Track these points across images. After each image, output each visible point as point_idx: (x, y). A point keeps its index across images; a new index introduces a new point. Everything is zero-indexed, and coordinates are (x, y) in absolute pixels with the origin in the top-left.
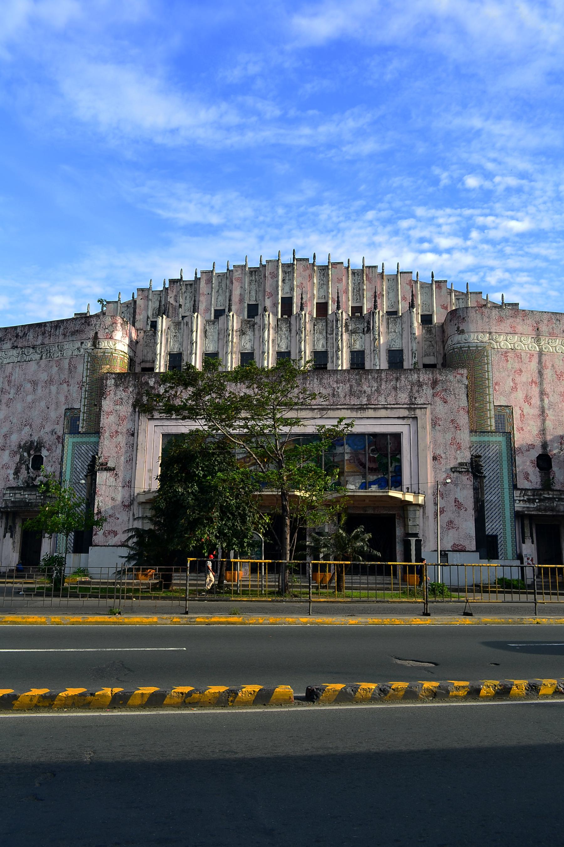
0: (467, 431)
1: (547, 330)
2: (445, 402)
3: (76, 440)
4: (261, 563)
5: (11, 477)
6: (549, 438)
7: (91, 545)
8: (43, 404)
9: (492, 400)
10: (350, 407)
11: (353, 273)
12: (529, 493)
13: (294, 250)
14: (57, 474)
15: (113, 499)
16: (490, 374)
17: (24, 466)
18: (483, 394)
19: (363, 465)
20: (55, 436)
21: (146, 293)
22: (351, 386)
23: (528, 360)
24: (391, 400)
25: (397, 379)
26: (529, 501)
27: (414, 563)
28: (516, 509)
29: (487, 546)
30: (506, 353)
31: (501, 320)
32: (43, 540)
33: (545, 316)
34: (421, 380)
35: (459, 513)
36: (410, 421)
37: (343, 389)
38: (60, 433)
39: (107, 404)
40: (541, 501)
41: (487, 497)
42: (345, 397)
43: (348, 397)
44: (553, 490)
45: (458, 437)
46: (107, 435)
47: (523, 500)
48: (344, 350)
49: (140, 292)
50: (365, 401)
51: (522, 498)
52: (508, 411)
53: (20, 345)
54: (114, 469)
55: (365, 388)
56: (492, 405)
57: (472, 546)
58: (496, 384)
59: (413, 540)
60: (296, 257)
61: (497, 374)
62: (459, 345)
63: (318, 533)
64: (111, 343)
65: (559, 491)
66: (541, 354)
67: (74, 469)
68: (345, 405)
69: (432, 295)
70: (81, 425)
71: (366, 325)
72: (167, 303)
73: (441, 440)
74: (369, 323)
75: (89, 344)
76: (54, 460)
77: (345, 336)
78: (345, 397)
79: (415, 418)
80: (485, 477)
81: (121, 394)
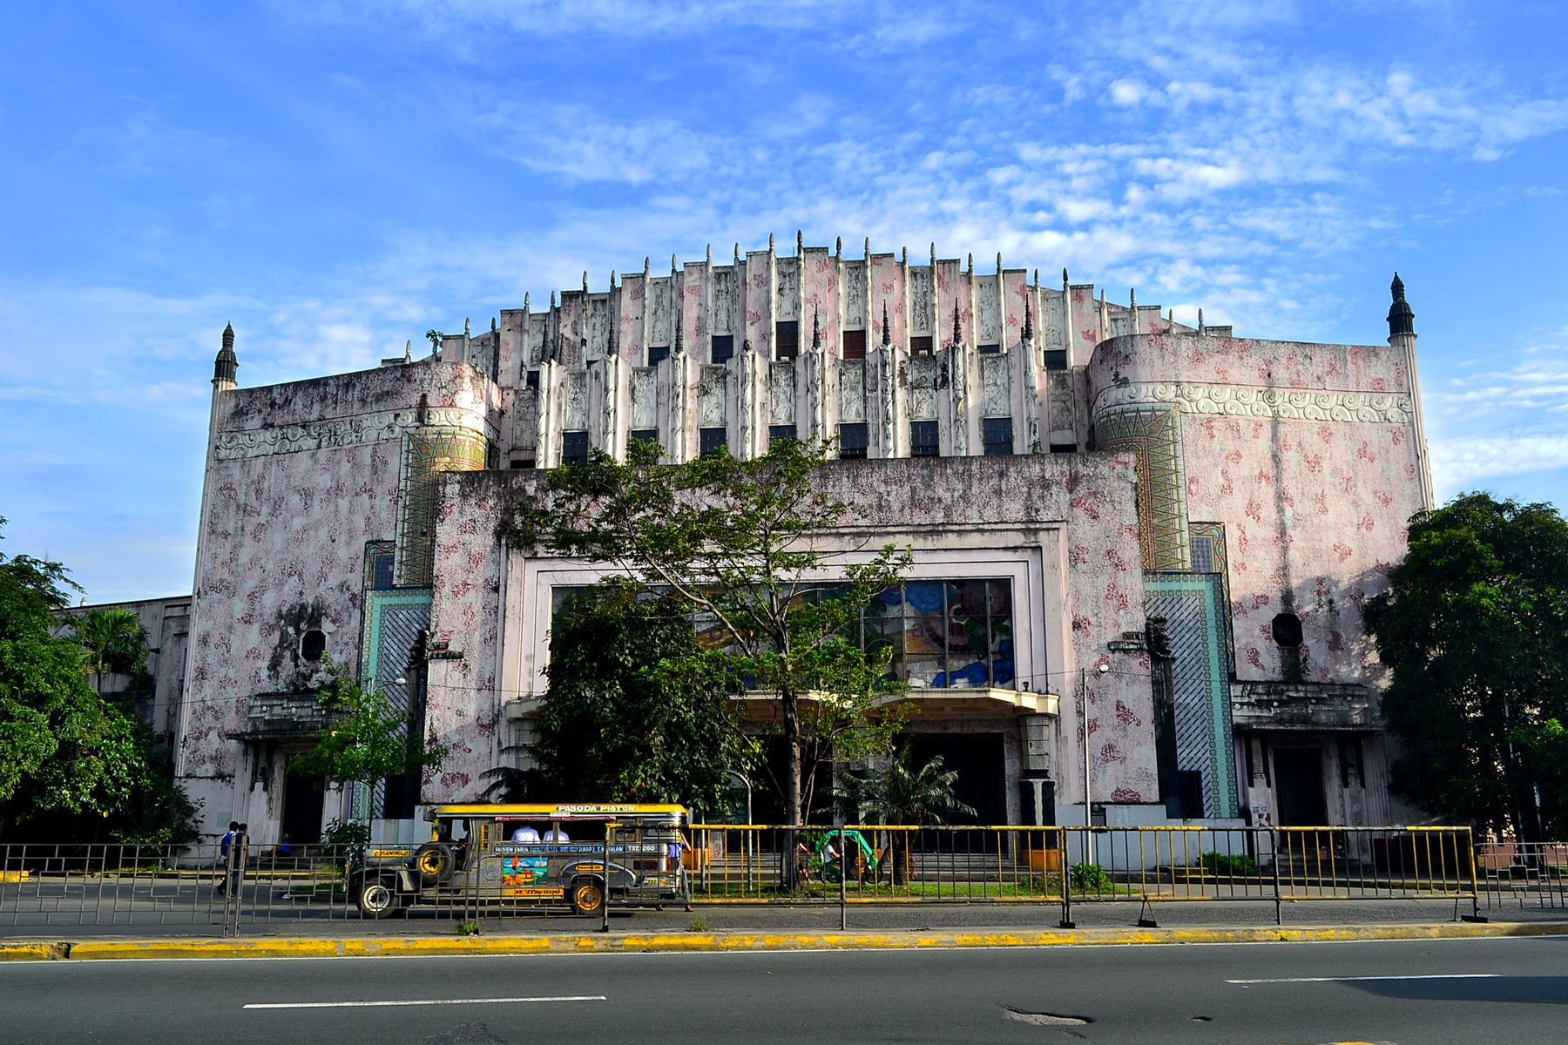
0: (1138, 572)
3: (387, 601)
4: (746, 831)
5: (264, 674)
6: (1295, 582)
7: (419, 803)
8: (323, 533)
9: (1183, 512)
11: (914, 274)
12: (1260, 689)
14: (353, 666)
15: (459, 713)
16: (1180, 462)
17: (288, 654)
18: (1167, 500)
19: (939, 641)
20: (347, 595)
21: (518, 319)
22: (913, 490)
24: (990, 514)
25: (1002, 475)
26: (1260, 704)
27: (1040, 826)
28: (1235, 720)
29: (1181, 793)
30: (1209, 421)
31: (1198, 358)
32: (327, 794)
33: (1283, 350)
34: (1047, 476)
35: (1125, 729)
36: (1027, 555)
37: (897, 496)
38: (357, 589)
39: (446, 532)
40: (1282, 703)
41: (1179, 698)
42: (902, 510)
43: (907, 511)
44: (1305, 683)
46: (446, 590)
47: (1248, 704)
48: (900, 420)
49: (507, 318)
50: (940, 517)
51: (1246, 700)
53: (278, 422)
54: (461, 656)
55: (940, 492)
56: (1184, 521)
57: (1154, 793)
58: (1191, 481)
59: (1038, 784)
61: (1193, 461)
62: (1118, 408)
63: (853, 773)
64: (453, 414)
65: (1318, 684)
66: (1276, 422)
67: (384, 658)
68: (902, 525)
69: (1065, 313)
70: (396, 572)
71: (939, 371)
72: (559, 337)
73: (1087, 589)
74: (945, 368)
75: (410, 418)
76: (345, 639)
77: (901, 394)
78: (902, 510)
80: (1174, 660)
81: (472, 511)
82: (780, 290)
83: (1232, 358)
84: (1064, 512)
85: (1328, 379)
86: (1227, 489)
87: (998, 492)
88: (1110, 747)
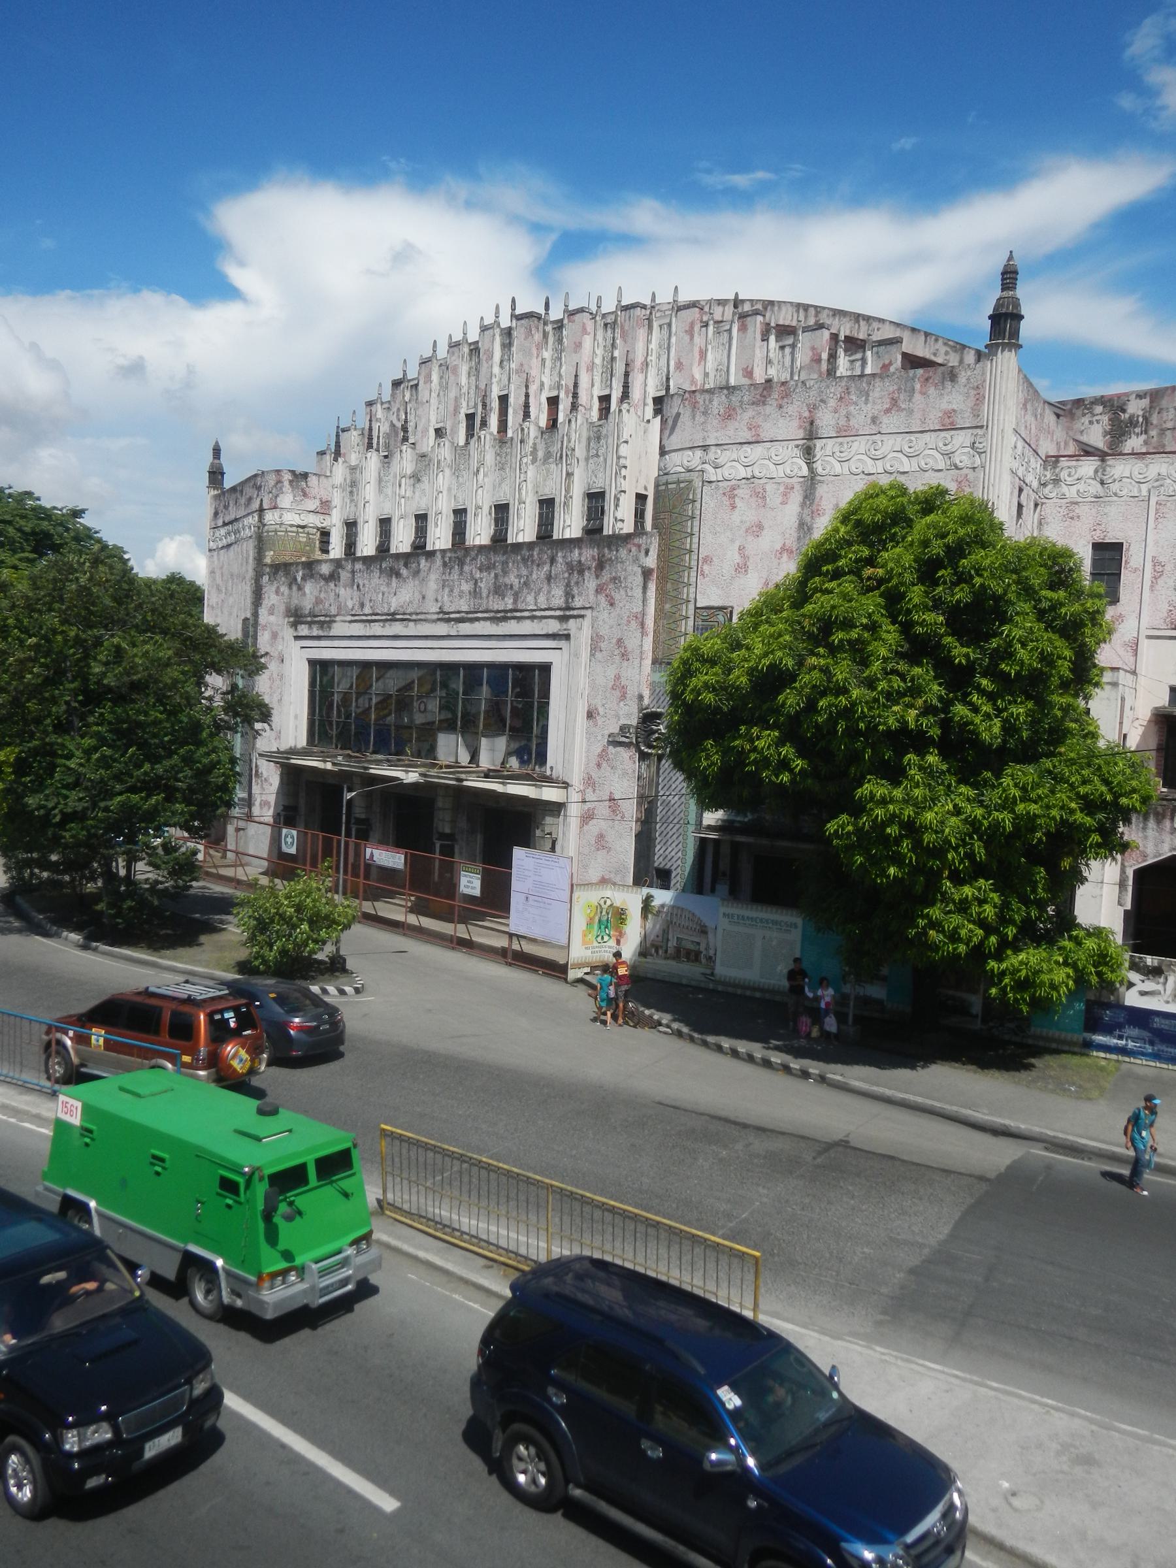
1: (833, 422)
2: (612, 605)
9: (692, 596)
10: (492, 614)
13: (513, 300)
16: (695, 540)
18: (679, 583)
22: (496, 576)
23: (780, 500)
24: (542, 601)
25: (553, 561)
31: (729, 415)
36: (562, 644)
42: (488, 597)
45: (623, 674)
50: (509, 603)
52: (721, 618)
56: (691, 606)
58: (706, 560)
60: (517, 312)
64: (277, 513)
66: (811, 481)
78: (488, 597)
79: (567, 637)
82: (501, 362)
83: (768, 409)
84: (592, 597)
85: (885, 420)
86: (742, 568)
87: (549, 578)
88: (601, 837)
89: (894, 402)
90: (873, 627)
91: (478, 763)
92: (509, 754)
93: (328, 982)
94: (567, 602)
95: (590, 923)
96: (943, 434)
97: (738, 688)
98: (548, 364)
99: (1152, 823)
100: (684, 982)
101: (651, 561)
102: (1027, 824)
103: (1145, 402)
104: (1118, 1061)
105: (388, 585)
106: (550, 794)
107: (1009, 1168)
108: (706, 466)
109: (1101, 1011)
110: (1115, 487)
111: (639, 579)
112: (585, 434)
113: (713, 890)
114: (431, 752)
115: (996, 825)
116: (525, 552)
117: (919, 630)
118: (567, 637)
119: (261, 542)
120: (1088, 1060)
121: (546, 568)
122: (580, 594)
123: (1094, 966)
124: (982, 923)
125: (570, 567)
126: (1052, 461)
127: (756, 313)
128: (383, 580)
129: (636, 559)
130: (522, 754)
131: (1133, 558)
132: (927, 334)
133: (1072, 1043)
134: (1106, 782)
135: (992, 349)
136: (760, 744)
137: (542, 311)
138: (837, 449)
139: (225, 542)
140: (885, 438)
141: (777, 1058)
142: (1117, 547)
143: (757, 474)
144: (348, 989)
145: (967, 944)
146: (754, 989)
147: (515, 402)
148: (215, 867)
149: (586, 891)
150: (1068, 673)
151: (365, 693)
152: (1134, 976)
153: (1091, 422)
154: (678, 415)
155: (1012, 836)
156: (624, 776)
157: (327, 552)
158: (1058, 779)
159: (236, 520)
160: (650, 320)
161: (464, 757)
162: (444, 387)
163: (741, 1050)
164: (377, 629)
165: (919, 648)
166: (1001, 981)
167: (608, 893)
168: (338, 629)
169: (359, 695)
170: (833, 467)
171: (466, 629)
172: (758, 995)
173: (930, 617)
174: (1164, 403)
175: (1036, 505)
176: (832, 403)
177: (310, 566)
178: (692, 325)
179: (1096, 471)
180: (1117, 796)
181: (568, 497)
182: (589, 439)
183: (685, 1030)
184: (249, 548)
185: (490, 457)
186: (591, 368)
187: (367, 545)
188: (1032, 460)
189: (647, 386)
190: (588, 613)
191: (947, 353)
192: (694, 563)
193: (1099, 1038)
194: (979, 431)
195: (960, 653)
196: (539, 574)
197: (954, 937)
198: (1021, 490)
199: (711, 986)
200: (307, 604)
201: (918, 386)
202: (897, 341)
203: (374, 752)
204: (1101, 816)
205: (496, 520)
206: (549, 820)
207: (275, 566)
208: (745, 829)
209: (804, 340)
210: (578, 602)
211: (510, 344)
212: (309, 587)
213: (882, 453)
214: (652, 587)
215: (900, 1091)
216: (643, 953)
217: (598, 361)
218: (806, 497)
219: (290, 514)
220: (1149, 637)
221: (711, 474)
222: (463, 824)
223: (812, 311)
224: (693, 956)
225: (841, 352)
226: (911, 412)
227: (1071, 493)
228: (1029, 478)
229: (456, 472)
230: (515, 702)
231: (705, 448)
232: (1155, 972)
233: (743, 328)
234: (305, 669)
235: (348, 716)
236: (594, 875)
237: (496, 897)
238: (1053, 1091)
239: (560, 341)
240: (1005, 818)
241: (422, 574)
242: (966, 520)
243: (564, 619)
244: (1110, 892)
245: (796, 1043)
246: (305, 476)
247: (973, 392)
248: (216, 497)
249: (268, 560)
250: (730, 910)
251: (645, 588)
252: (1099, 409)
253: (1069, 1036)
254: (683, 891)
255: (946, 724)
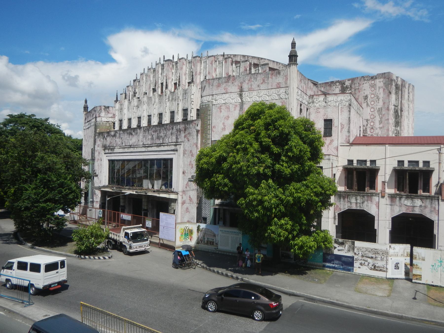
1: (247, 87)
9: (210, 137)
13: (164, 56)
16: (211, 121)
22: (158, 134)
24: (170, 141)
25: (173, 129)
31: (219, 86)
36: (175, 152)
50: (161, 141)
56: (210, 140)
58: (214, 127)
64: (100, 118)
66: (242, 103)
79: (177, 150)
83: (229, 84)
84: (183, 139)
85: (261, 86)
86: (224, 129)
87: (172, 134)
88: (187, 208)
89: (264, 81)
90: (251, 144)
91: (152, 188)
92: (162, 185)
93: (101, 255)
94: (176, 140)
95: (182, 234)
96: (277, 89)
97: (213, 163)
98: (174, 74)
99: (342, 200)
100: (210, 251)
101: (199, 128)
102: (297, 201)
103: (350, 82)
104: (333, 271)
105: (129, 137)
106: (172, 196)
107: (290, 306)
108: (213, 100)
109: (328, 256)
110: (329, 103)
111: (196, 133)
112: (182, 93)
113: (218, 223)
114: (141, 185)
115: (288, 201)
116: (165, 127)
117: (264, 143)
118: (177, 150)
119: (96, 127)
120: (324, 271)
121: (171, 131)
122: (180, 138)
123: (323, 242)
124: (286, 230)
125: (177, 130)
126: (311, 97)
127: (229, 58)
128: (128, 135)
129: (195, 127)
130: (166, 185)
131: (335, 123)
132: (277, 62)
133: (319, 266)
134: (322, 187)
135: (289, 65)
136: (218, 179)
137: (172, 59)
138: (248, 94)
139: (88, 127)
140: (261, 91)
141: (230, 273)
142: (331, 121)
143: (227, 102)
144: (106, 257)
145: (283, 237)
146: (229, 253)
147: (164, 84)
148: (81, 221)
149: (182, 225)
150: (310, 156)
151: (124, 169)
152: (336, 245)
153: (336, 88)
154: (205, 86)
155: (292, 205)
156: (193, 191)
157: (114, 128)
158: (307, 187)
159: (90, 120)
160: (201, 61)
161: (150, 187)
162: (146, 81)
163: (220, 271)
164: (126, 150)
165: (264, 149)
166: (294, 247)
167: (187, 225)
168: (116, 150)
169: (122, 169)
170: (248, 99)
171: (150, 149)
172: (230, 254)
173: (267, 139)
174: (355, 82)
175: (307, 109)
176: (247, 81)
177: (108, 133)
178: (212, 61)
179: (324, 99)
180: (325, 191)
181: (178, 111)
182: (183, 94)
183: (205, 266)
184: (93, 128)
185: (157, 100)
186: (185, 74)
187: (125, 126)
188: (305, 96)
189: (199, 79)
190: (182, 143)
191: (282, 67)
192: (210, 128)
193: (328, 264)
194: (287, 88)
195: (276, 150)
196: (169, 133)
197: (279, 236)
198: (301, 105)
199: (217, 252)
200: (108, 144)
201: (270, 76)
202: (268, 64)
203: (126, 186)
204: (321, 197)
205: (159, 118)
206: (173, 204)
207: (101, 133)
208: (227, 205)
209: (242, 65)
210: (179, 140)
211: (164, 68)
212: (108, 139)
213: (260, 94)
214: (199, 135)
215: (264, 282)
216: (198, 243)
217: (187, 72)
218: (241, 108)
219: (104, 118)
220: (341, 146)
221: (215, 102)
222: (150, 206)
223: (246, 57)
224: (212, 243)
225: (252, 68)
226: (268, 83)
227: (317, 105)
228: (304, 102)
229: (148, 105)
230: (162, 170)
231: (213, 95)
232: (342, 244)
233: (226, 62)
234: (107, 163)
235: (119, 176)
236: (186, 220)
237: (156, 228)
238: (311, 281)
239: (177, 67)
240: (291, 199)
241: (138, 134)
242: (278, 112)
243: (176, 145)
244: (331, 221)
245: (237, 269)
246: (108, 107)
247: (285, 77)
248: (86, 114)
249: (98, 132)
250: (222, 229)
251: (197, 135)
252: (338, 84)
253: (319, 264)
254: (210, 224)
255: (273, 171)
